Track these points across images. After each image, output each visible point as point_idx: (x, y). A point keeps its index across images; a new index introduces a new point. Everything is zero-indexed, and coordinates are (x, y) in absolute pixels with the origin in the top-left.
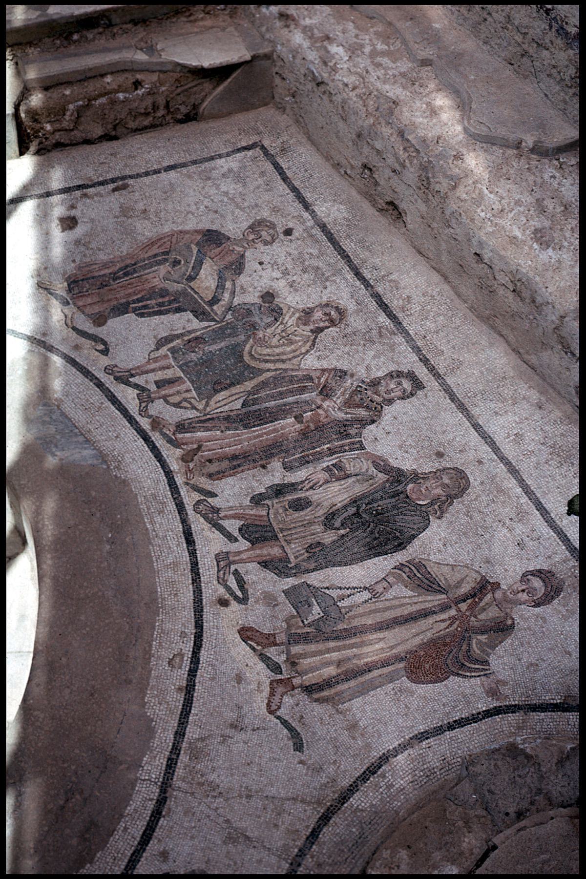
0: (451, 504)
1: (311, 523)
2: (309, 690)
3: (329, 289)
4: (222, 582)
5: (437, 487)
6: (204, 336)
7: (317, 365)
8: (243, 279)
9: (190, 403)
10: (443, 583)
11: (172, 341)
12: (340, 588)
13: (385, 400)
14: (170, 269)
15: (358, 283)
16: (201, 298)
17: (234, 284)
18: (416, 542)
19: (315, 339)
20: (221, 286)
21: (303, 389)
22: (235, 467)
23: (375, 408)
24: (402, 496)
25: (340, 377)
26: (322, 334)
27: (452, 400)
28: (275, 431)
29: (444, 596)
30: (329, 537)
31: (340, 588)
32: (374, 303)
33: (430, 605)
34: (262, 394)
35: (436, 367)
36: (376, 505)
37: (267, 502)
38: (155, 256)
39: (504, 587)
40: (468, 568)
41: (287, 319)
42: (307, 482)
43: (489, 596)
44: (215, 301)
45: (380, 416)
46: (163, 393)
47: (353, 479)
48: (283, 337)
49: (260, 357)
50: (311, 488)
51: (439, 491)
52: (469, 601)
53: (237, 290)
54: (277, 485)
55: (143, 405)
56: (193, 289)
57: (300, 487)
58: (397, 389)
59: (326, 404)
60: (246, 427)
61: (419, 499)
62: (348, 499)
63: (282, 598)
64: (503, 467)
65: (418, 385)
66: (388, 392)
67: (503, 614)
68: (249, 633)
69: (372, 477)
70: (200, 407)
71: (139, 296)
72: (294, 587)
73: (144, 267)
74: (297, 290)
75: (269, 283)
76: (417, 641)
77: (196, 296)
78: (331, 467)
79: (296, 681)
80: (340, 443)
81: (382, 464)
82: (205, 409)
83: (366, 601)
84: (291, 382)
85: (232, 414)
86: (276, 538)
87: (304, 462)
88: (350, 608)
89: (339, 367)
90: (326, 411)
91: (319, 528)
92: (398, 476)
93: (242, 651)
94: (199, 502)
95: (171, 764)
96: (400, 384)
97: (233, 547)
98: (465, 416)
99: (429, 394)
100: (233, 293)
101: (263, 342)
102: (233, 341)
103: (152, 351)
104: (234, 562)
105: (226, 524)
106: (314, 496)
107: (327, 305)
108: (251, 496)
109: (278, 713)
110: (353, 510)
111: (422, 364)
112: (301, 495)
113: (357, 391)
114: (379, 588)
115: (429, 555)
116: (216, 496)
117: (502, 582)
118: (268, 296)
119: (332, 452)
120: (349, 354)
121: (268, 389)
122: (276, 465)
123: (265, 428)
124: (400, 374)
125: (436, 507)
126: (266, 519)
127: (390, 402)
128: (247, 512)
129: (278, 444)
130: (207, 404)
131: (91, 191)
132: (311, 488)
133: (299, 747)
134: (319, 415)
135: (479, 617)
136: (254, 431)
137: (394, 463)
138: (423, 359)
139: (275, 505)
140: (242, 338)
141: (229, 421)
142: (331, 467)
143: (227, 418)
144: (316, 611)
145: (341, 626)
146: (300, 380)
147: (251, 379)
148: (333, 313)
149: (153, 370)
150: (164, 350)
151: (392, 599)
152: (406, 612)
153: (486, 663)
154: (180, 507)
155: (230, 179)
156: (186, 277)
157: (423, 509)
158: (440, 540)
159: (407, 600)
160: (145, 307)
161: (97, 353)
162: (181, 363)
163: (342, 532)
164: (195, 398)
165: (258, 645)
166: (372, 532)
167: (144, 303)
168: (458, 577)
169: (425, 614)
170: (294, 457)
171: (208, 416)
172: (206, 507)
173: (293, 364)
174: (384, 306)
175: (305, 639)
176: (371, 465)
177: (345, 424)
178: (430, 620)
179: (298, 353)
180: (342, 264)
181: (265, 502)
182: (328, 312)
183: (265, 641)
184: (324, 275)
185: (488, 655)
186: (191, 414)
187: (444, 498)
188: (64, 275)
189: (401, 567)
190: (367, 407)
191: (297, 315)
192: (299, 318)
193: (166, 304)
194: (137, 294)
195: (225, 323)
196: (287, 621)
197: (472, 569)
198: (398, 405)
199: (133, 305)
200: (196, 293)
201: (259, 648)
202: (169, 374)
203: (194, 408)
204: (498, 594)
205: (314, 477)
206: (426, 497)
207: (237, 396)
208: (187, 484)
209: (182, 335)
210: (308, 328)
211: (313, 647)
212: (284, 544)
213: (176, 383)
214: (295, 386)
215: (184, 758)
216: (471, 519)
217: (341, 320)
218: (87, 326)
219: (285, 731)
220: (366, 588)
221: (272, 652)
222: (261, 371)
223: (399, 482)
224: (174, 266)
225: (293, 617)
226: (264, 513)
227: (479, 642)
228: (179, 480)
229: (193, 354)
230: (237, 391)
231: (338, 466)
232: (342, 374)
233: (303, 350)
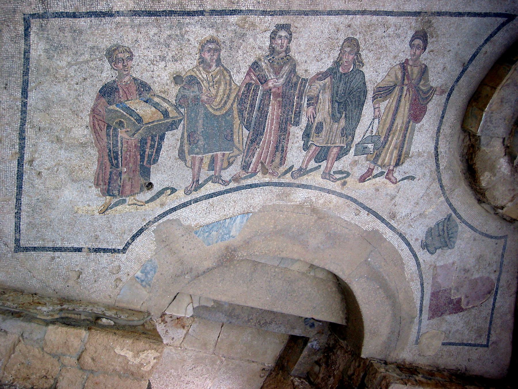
1: (331, 128)
2: (397, 165)
3: (190, 38)
5: (348, 56)
6: (189, 131)
7: (242, 76)
8: (156, 88)
9: (232, 157)
10: (392, 84)
12: (367, 130)
13: (286, 51)
14: (124, 130)
15: (196, 18)
16: (158, 121)
17: (158, 96)
19: (223, 67)
20: (156, 105)
22: (283, 150)
23: (287, 59)
25: (257, 67)
26: (222, 61)
27: (307, 15)
28: (272, 120)
29: (397, 87)
30: (343, 123)
31: (367, 130)
32: (217, 17)
34: (246, 115)
35: (282, 9)
36: (339, 92)
38: (108, 135)
39: (409, 58)
40: (392, 68)
41: (200, 76)
42: (310, 119)
43: (409, 67)
44: (166, 114)
45: (294, 60)
48: (213, 85)
49: (220, 106)
50: (314, 118)
51: (351, 57)
52: (405, 78)
53: (163, 96)
56: (149, 123)
57: (311, 124)
58: (283, 41)
59: (270, 84)
60: (262, 134)
61: (349, 69)
62: (330, 103)
63: (356, 158)
64: (359, 16)
66: (282, 46)
67: (419, 67)
69: (325, 85)
71: (139, 157)
72: (355, 150)
73: (115, 145)
74: (182, 59)
75: (166, 73)
76: (407, 110)
77: (155, 123)
78: (308, 103)
79: (391, 168)
80: (297, 90)
81: (321, 76)
82: (239, 150)
85: (251, 138)
86: (329, 148)
87: (298, 114)
89: (250, 64)
90: (275, 87)
91: (336, 125)
92: (331, 72)
94: (292, 176)
96: (280, 37)
98: (320, 15)
99: (296, 25)
100: (164, 99)
101: (211, 99)
103: (186, 164)
104: (330, 171)
105: (309, 167)
106: (319, 118)
107: (203, 47)
108: (302, 149)
111: (275, 16)
112: (315, 125)
113: (271, 63)
114: (377, 113)
115: (376, 82)
118: (177, 79)
119: (300, 97)
120: (245, 53)
121: (244, 111)
122: (293, 129)
123: (268, 125)
124: (274, 33)
125: (357, 63)
126: (318, 148)
127: (288, 50)
129: (281, 122)
131: (27, 157)
132: (314, 118)
133: (412, 178)
134: (275, 92)
136: (267, 131)
137: (325, 69)
138: (273, 13)
139: (313, 140)
141: (254, 140)
142: (308, 103)
143: (252, 141)
144: (371, 146)
145: (382, 139)
146: (248, 90)
150: (189, 158)
151: (385, 111)
152: (394, 108)
153: (432, 87)
155: (56, 55)
156: (136, 123)
157: (355, 70)
158: (373, 72)
159: (389, 105)
160: (150, 156)
162: (202, 151)
164: (230, 153)
165: (369, 177)
166: (352, 102)
168: (393, 76)
170: (293, 118)
171: (246, 151)
172: (296, 174)
173: (235, 89)
174: (222, 13)
175: (378, 156)
176: (319, 82)
177: (288, 82)
178: (403, 100)
179: (228, 82)
180: (175, 19)
181: (309, 144)
182: (208, 49)
183: (369, 173)
184: (177, 35)
185: (429, 84)
187: (355, 57)
188: (100, 196)
189: (374, 98)
191: (201, 69)
192: (204, 69)
193: (153, 143)
194: (137, 158)
195: (186, 115)
196: (367, 160)
197: (394, 67)
198: (293, 46)
199: (145, 164)
200: (153, 122)
202: (206, 162)
203: (236, 156)
204: (410, 63)
205: (309, 114)
206: (350, 65)
207: (241, 130)
209: (182, 143)
210: (214, 67)
211: (383, 155)
212: (333, 145)
213: (215, 159)
214: (250, 96)
216: (373, 51)
217: (218, 44)
218: (148, 195)
220: (374, 119)
221: (375, 172)
222: (231, 108)
223: (336, 73)
224: (123, 127)
225: (367, 157)
226: (314, 147)
227: (423, 85)
229: (200, 143)
230: (237, 129)
233: (228, 78)
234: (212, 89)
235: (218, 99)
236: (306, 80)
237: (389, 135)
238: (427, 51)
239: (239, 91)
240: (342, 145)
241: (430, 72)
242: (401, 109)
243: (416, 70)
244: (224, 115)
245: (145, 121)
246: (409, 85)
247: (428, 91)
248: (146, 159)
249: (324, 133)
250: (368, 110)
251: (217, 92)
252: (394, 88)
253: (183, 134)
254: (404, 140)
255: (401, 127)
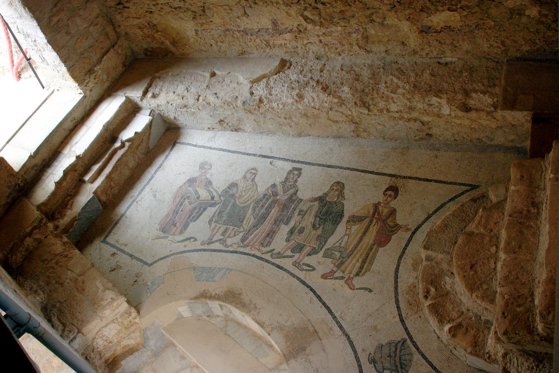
0: (344, 193)
1: (310, 233)
2: (357, 274)
4: (302, 270)
11: (212, 220)
17: (213, 188)
18: (345, 212)
19: (255, 182)
20: (210, 192)
21: (267, 200)
24: (328, 203)
28: (272, 217)
29: (368, 218)
30: (319, 232)
33: (366, 224)
37: (291, 238)
38: (180, 201)
39: (381, 201)
43: (380, 207)
44: (213, 198)
46: (226, 236)
47: (309, 210)
51: (337, 193)
52: (376, 213)
54: (289, 231)
55: (224, 244)
59: (278, 198)
60: (262, 224)
61: (333, 199)
65: (299, 170)
66: (293, 179)
68: (325, 276)
70: (242, 229)
72: (324, 253)
79: (352, 276)
83: (348, 239)
84: (261, 201)
87: (289, 219)
88: (346, 244)
91: (314, 232)
92: (321, 199)
93: (329, 282)
94: (271, 255)
95: (341, 327)
96: (294, 174)
97: (295, 259)
102: (231, 204)
105: (286, 254)
106: (303, 224)
109: (355, 288)
110: (318, 219)
112: (299, 228)
116: (274, 249)
117: (380, 201)
119: (294, 209)
127: (296, 181)
128: (288, 246)
130: (244, 228)
132: (300, 223)
135: (383, 215)
137: (316, 196)
140: (233, 201)
141: (255, 226)
143: (254, 226)
145: (348, 251)
146: (264, 197)
147: (249, 209)
148: (252, 171)
149: (216, 232)
150: (213, 225)
152: (363, 231)
153: (397, 225)
154: (267, 261)
159: (359, 229)
161: (193, 243)
163: (321, 227)
167: (192, 217)
169: (367, 228)
175: (342, 263)
178: (371, 227)
183: (332, 274)
185: (396, 222)
186: (242, 234)
189: (348, 221)
190: (291, 188)
196: (332, 263)
198: (300, 180)
201: (332, 277)
202: (222, 229)
204: (382, 204)
208: (263, 254)
210: (249, 182)
212: (308, 245)
215: (342, 322)
219: (362, 291)
220: (344, 236)
221: (336, 275)
224: (189, 199)
226: (294, 242)
228: (259, 254)
231: (301, 211)
232: (274, 186)
233: (255, 189)
234: (243, 192)
235: (244, 198)
236: (301, 200)
237: (355, 250)
238: (397, 199)
239: (258, 197)
240: (315, 246)
241: (397, 214)
242: (368, 234)
243: (386, 211)
244: (244, 207)
245: (201, 199)
246: (378, 220)
247: (395, 227)
248: (191, 218)
249: (303, 234)
250: (341, 228)
251: (246, 194)
252: (365, 218)
253: (216, 211)
254: (367, 257)
255: (366, 247)
